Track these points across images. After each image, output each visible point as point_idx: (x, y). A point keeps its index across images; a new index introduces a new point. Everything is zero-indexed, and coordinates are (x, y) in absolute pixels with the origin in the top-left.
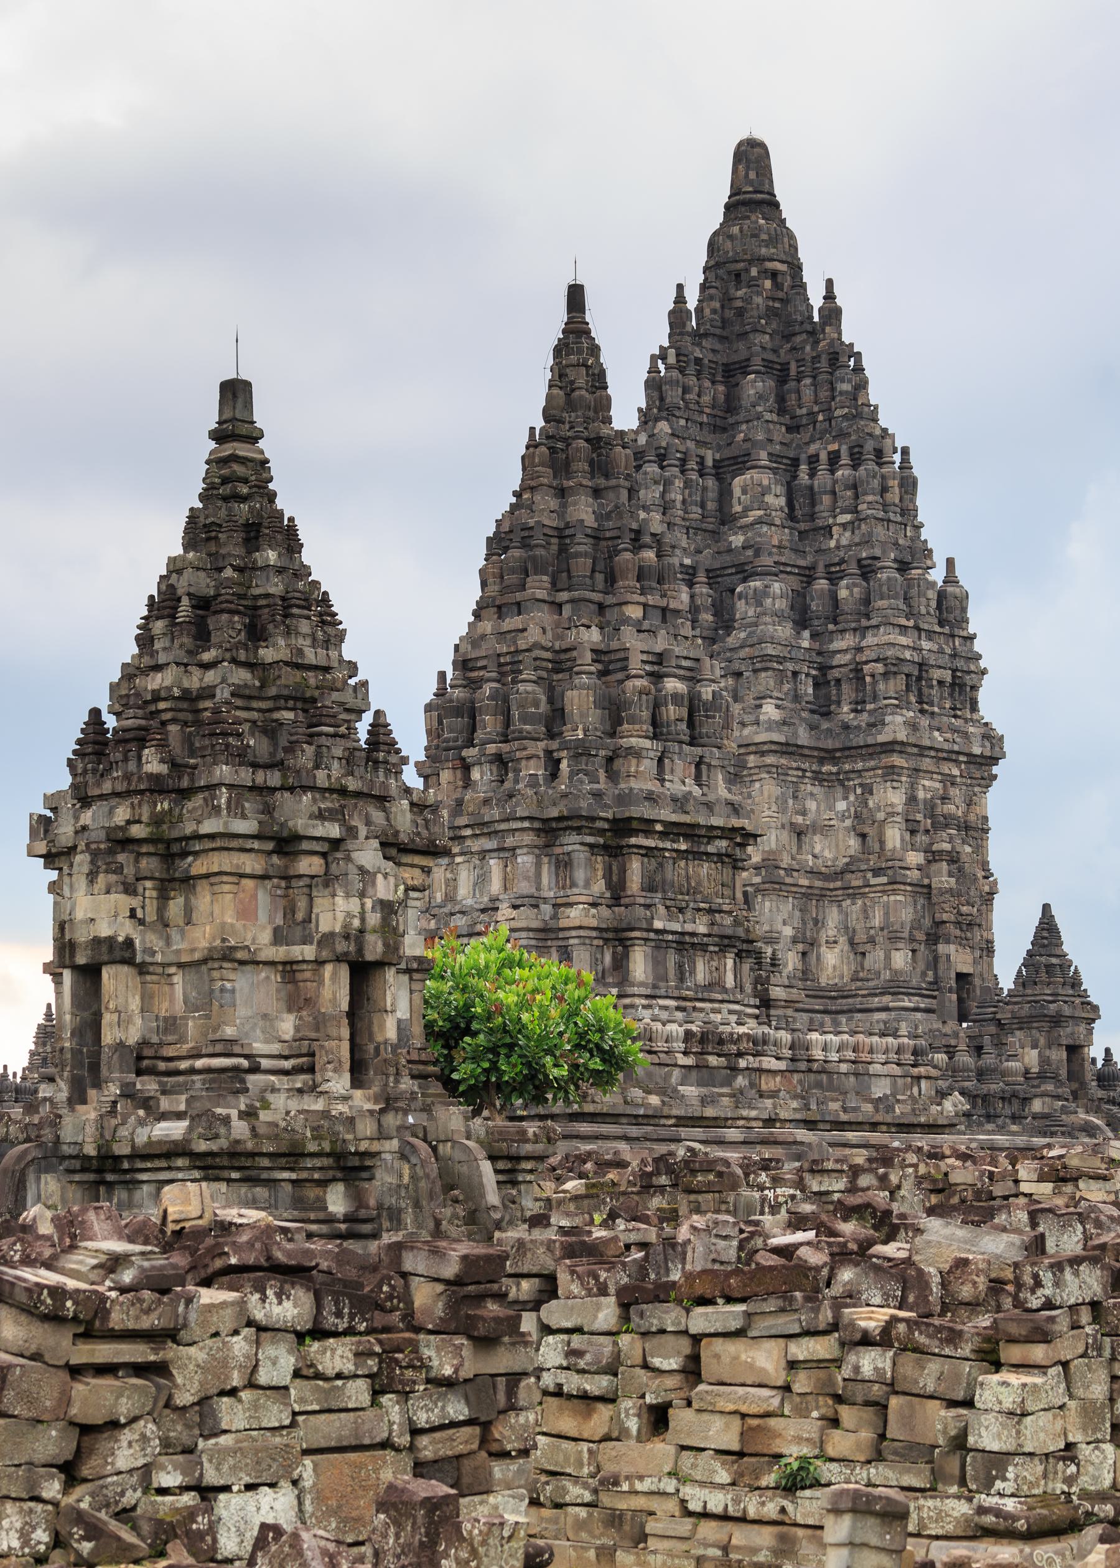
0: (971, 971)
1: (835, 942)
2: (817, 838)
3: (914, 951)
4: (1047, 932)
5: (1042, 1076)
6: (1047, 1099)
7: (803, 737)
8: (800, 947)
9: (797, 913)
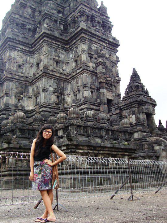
0: (112, 99)
1: (70, 94)
2: (64, 65)
3: (92, 92)
4: (135, 77)
5: (137, 124)
6: (139, 133)
7: (57, 34)
8: (56, 94)
9: (55, 84)
